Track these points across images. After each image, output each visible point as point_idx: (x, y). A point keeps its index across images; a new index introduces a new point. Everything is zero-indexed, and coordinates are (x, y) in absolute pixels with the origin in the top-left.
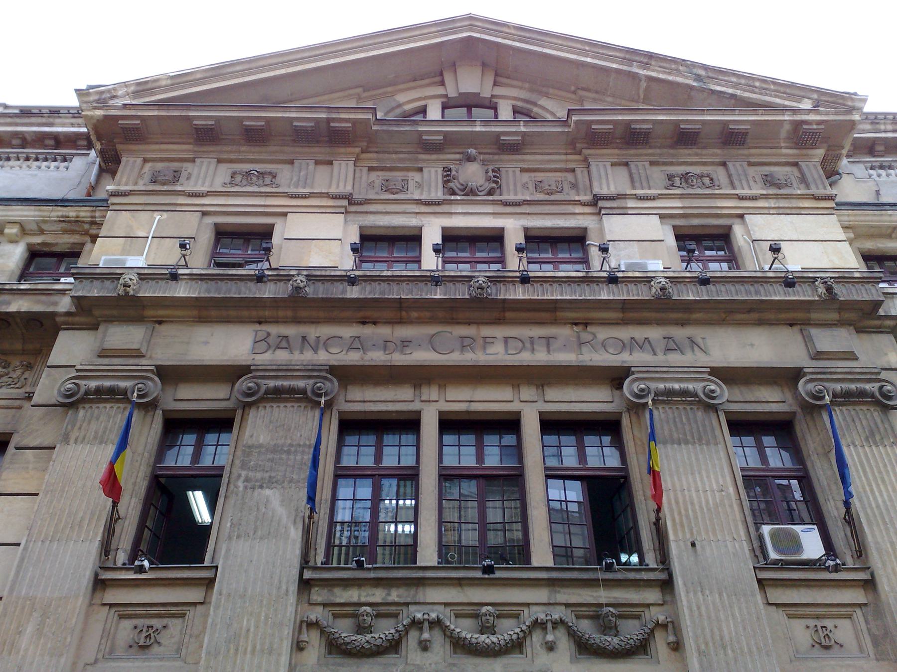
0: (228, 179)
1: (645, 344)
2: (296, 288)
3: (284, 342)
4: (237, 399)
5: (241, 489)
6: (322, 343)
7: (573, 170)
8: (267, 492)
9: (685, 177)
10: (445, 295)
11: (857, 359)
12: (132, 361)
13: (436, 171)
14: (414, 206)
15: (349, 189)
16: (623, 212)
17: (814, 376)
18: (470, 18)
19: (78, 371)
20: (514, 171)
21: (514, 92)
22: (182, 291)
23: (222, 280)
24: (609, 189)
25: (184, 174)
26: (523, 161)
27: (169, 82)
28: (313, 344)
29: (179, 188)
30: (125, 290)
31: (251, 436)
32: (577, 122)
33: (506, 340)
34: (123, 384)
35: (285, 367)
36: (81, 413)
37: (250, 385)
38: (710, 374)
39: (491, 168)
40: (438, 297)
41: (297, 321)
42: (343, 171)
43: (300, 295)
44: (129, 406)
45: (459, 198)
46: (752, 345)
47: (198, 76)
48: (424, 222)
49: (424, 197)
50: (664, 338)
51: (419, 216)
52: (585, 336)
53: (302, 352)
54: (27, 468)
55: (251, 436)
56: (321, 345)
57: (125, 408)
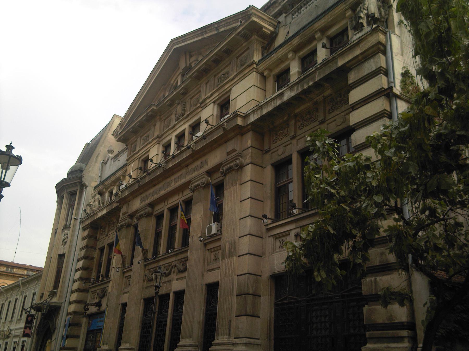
11: (236, 150)
18: (172, 41)
27: (124, 120)
47: (128, 114)
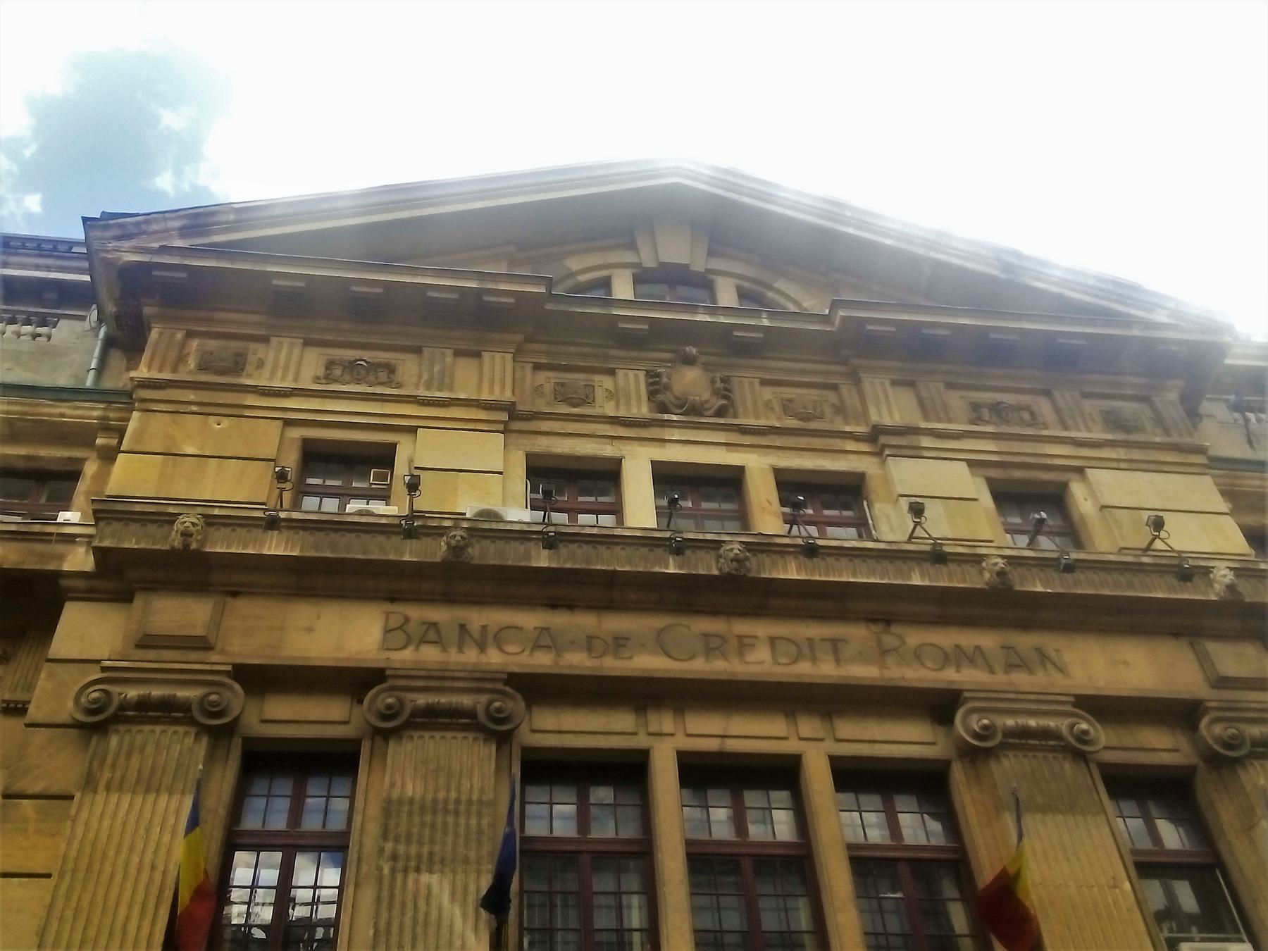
0: (321, 372)
1: (975, 657)
2: (454, 548)
3: (432, 634)
4: (370, 724)
5: (386, 871)
6: (491, 635)
7: (835, 387)
8: (425, 878)
9: (996, 408)
10: (680, 569)
12: (193, 656)
13: (636, 376)
14: (607, 427)
15: (508, 396)
16: (916, 453)
17: (1221, 714)
19: (104, 669)
20: (751, 384)
21: (738, 268)
22: (275, 546)
23: (336, 531)
24: (891, 416)
25: (252, 359)
28: (476, 635)
29: (249, 382)
30: (184, 540)
31: (393, 785)
32: (844, 319)
33: (773, 641)
34: (183, 693)
35: (439, 674)
36: (114, 741)
37: (390, 700)
38: (1075, 705)
39: (718, 375)
40: (672, 570)
41: (449, 598)
42: (498, 368)
43: (461, 559)
44: (193, 730)
45: (675, 418)
46: (1126, 663)
48: (624, 452)
49: (622, 413)
50: (1003, 648)
51: (615, 442)
52: (889, 640)
53: (460, 650)
54: (26, 830)
55: (393, 785)
56: (490, 640)
57: (186, 733)
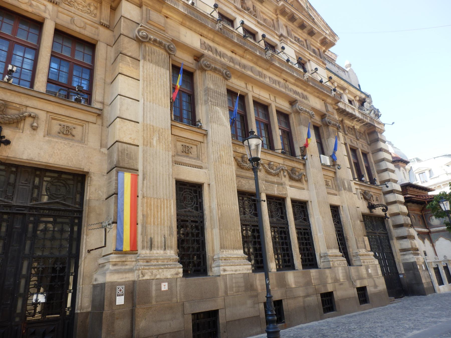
12: (162, 32)
26: (262, 8)
